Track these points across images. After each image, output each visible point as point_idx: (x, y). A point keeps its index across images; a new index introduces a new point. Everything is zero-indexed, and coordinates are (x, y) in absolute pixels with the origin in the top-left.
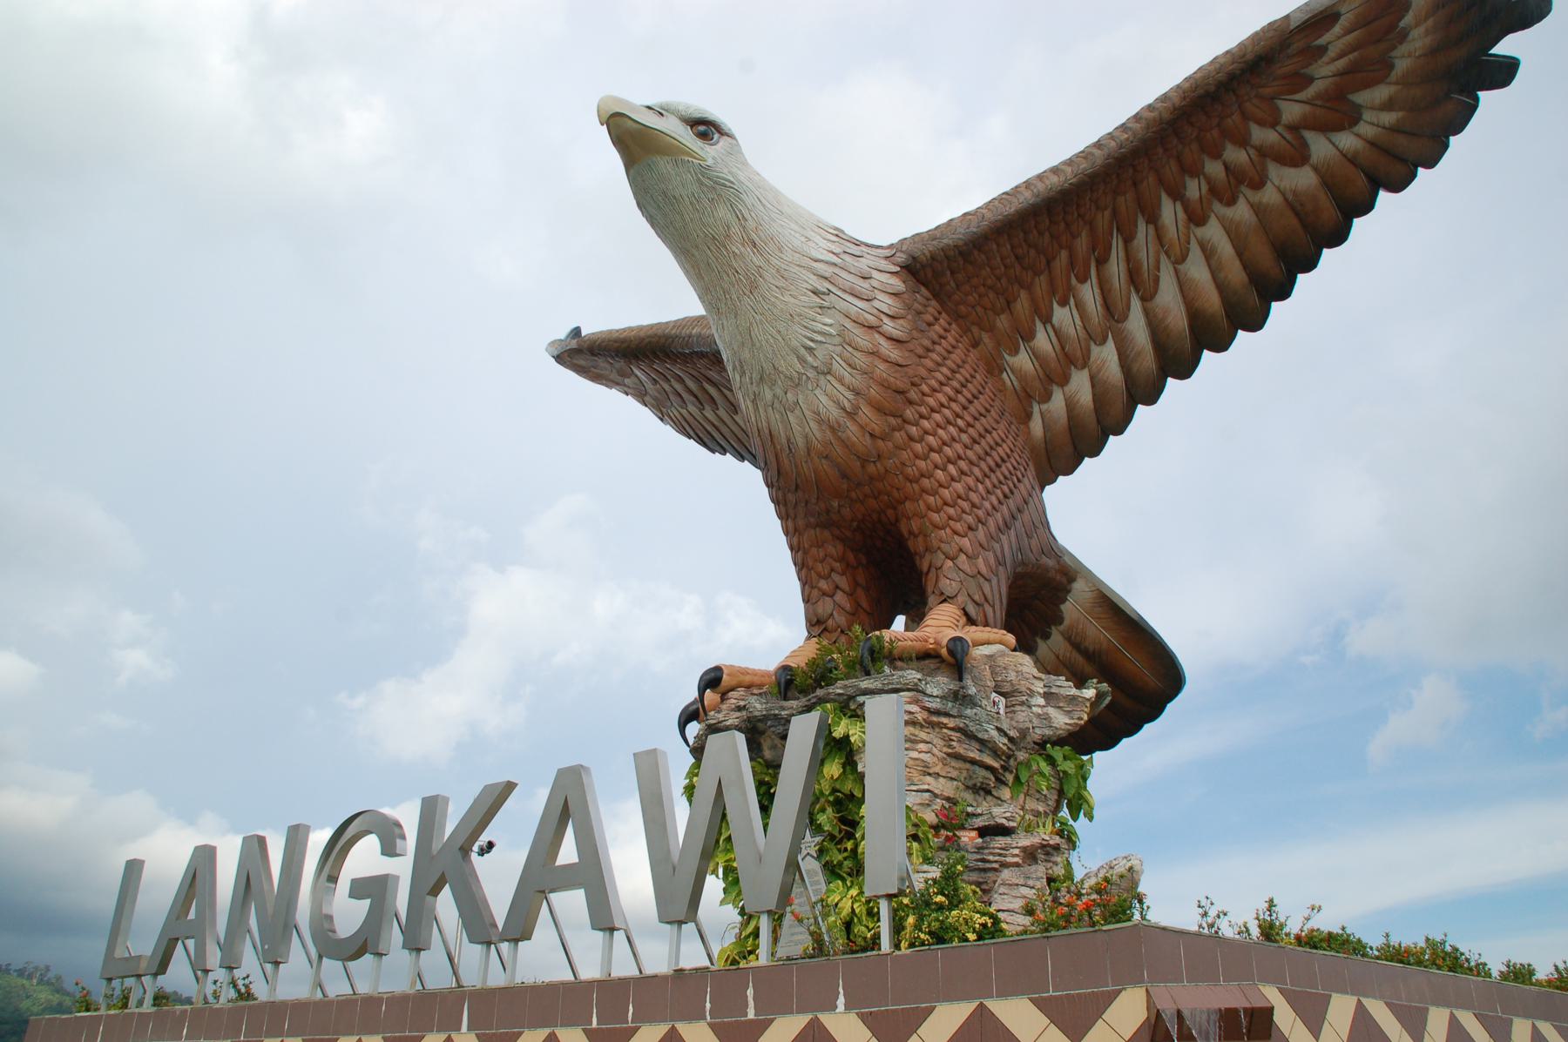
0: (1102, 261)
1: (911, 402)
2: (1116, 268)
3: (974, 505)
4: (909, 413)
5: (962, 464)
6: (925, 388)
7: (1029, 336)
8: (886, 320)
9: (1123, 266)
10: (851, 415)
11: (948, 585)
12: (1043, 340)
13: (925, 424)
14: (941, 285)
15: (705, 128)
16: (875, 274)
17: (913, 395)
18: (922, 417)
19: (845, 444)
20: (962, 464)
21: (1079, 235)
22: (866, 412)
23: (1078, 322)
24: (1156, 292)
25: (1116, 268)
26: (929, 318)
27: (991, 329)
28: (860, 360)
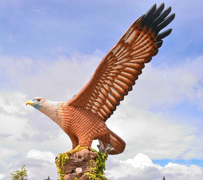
1: (71, 122)
3: (82, 132)
4: (72, 124)
5: (80, 127)
6: (73, 120)
8: (66, 114)
9: (104, 91)
11: (80, 142)
13: (74, 124)
14: (75, 105)
15: (39, 100)
16: (64, 108)
17: (72, 121)
18: (73, 124)
20: (80, 127)
21: (94, 90)
22: (67, 125)
23: (100, 100)
24: (111, 91)
26: (73, 110)
27: (87, 106)
28: (64, 120)
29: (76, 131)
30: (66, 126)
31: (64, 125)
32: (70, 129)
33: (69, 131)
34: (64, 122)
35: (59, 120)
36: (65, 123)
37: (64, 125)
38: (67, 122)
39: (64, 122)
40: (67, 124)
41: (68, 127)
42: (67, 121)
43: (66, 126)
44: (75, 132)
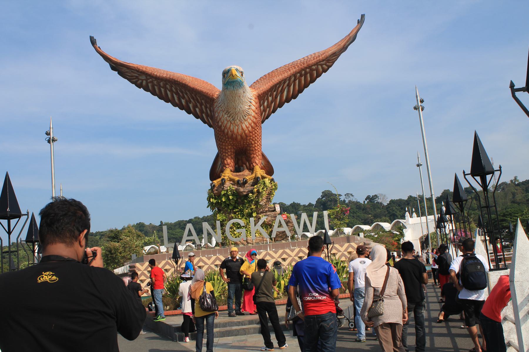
0: (279, 88)
2: (280, 89)
7: (264, 103)
10: (247, 128)
12: (266, 104)
19: (245, 134)
22: (250, 129)
25: (280, 89)
28: (252, 118)
29: (256, 142)
30: (248, 130)
31: (246, 126)
32: (250, 136)
33: (246, 138)
34: (250, 121)
35: (247, 117)
36: (250, 124)
37: (246, 126)
38: (253, 124)
39: (250, 121)
40: (252, 127)
41: (250, 132)
42: (254, 123)
43: (248, 130)
44: (253, 142)
